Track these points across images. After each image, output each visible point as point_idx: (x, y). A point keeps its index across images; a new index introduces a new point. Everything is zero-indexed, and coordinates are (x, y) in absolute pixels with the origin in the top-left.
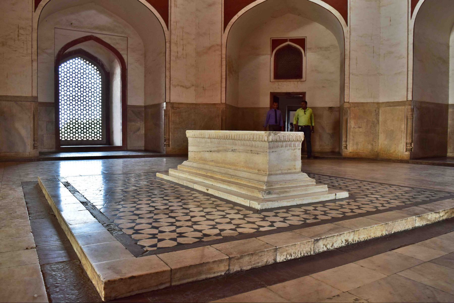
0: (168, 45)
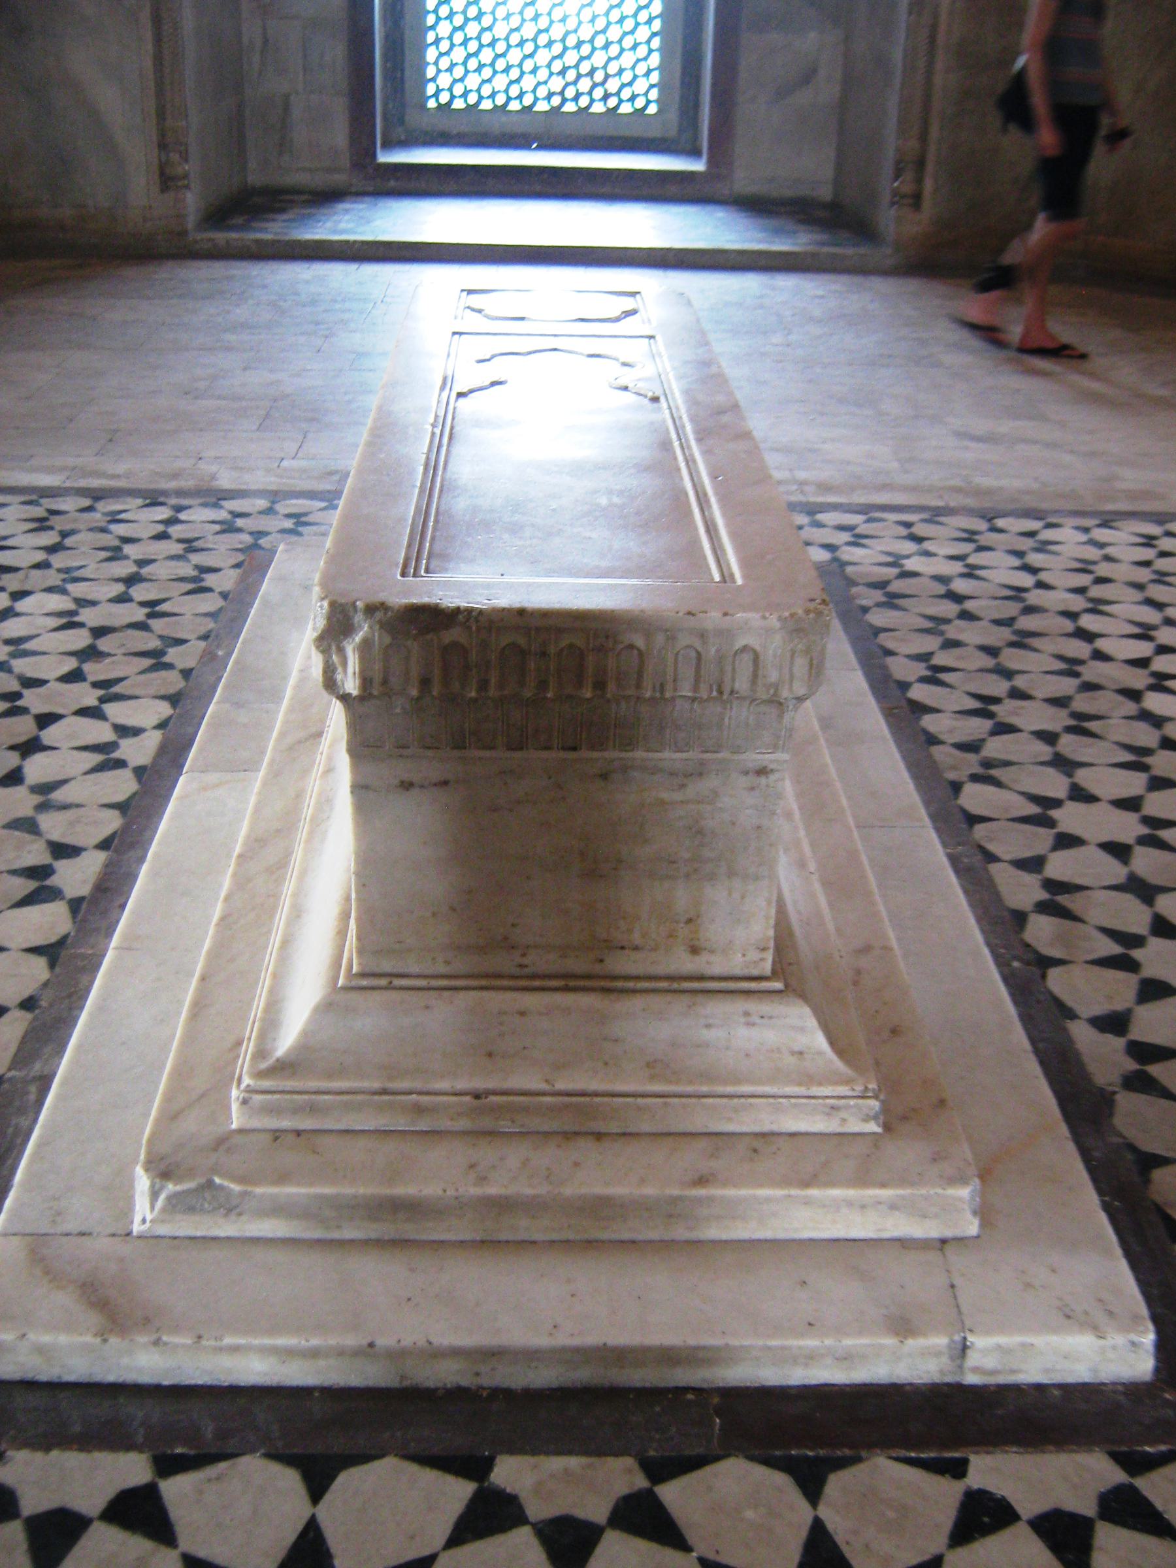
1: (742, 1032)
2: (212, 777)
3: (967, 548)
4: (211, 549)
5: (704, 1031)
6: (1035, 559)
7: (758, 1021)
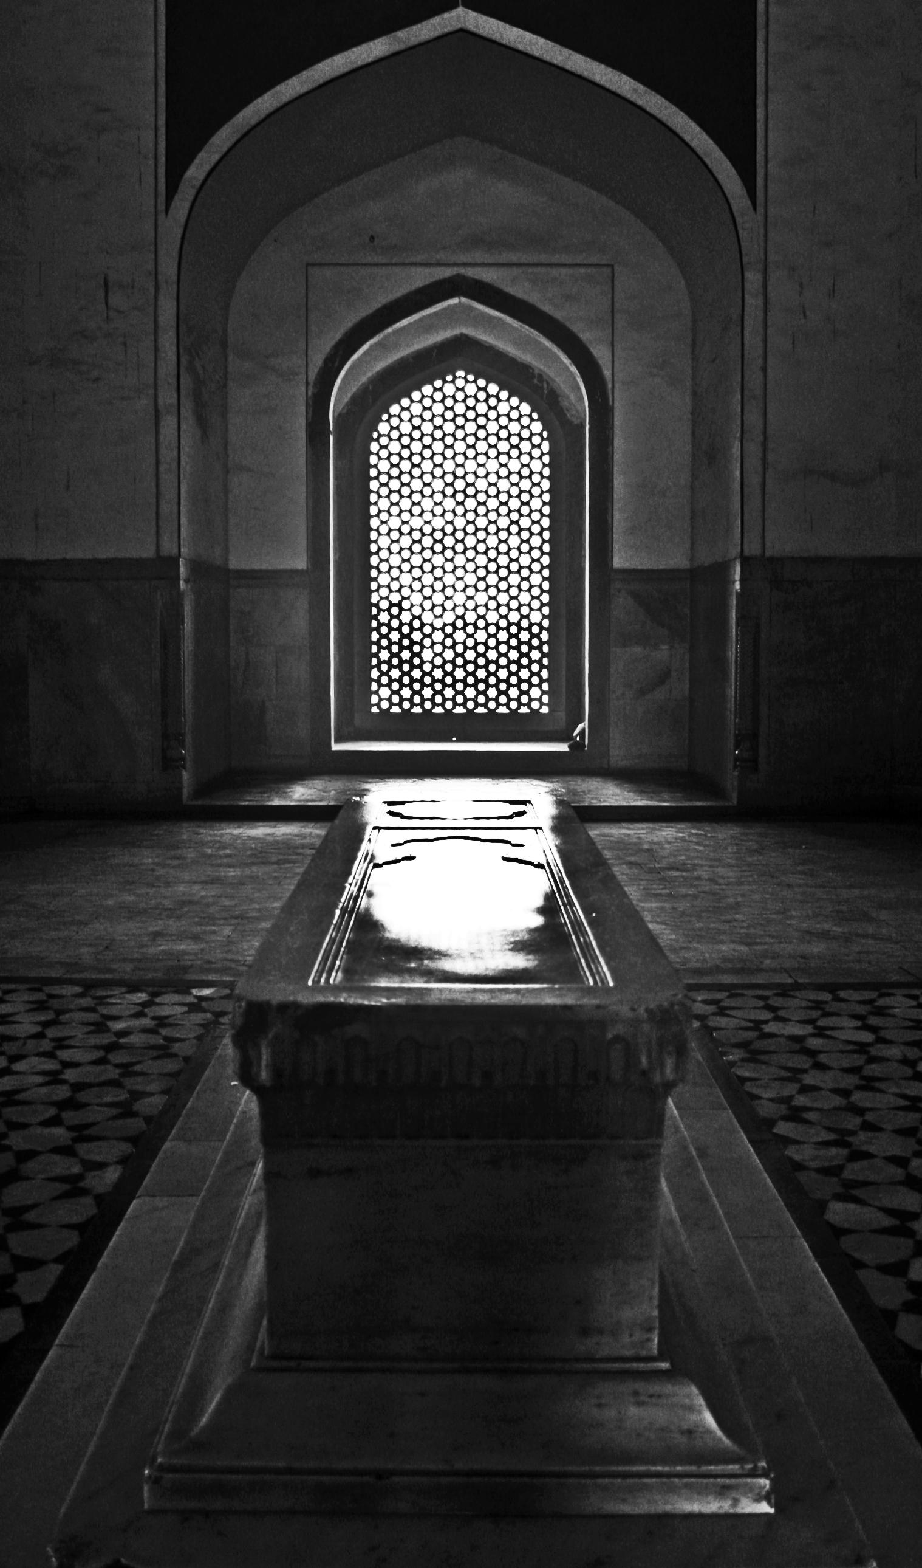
0: (753, 278)
1: (633, 1411)
2: (159, 1202)
3: (815, 1014)
4: (177, 1025)
5: (595, 1412)
6: (873, 1021)
7: (648, 1400)
